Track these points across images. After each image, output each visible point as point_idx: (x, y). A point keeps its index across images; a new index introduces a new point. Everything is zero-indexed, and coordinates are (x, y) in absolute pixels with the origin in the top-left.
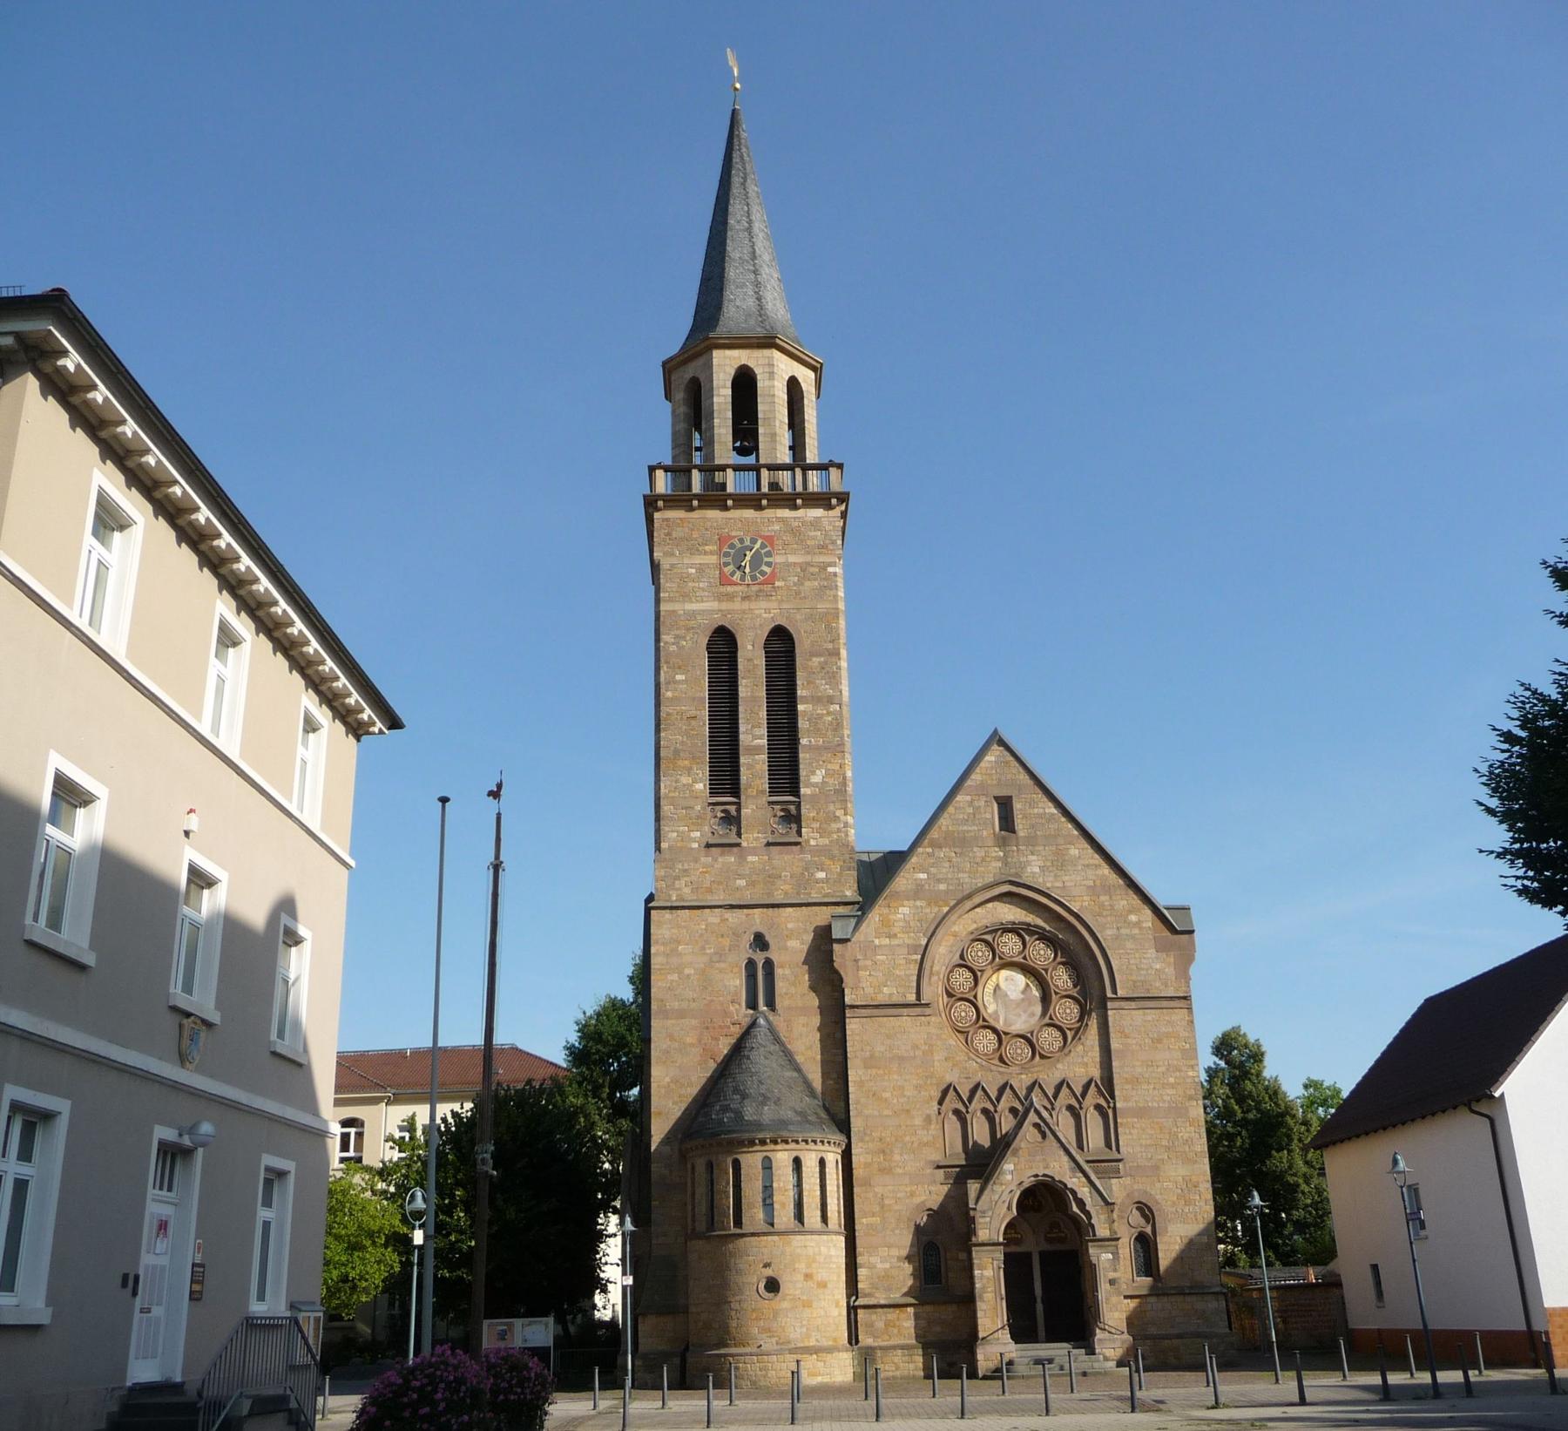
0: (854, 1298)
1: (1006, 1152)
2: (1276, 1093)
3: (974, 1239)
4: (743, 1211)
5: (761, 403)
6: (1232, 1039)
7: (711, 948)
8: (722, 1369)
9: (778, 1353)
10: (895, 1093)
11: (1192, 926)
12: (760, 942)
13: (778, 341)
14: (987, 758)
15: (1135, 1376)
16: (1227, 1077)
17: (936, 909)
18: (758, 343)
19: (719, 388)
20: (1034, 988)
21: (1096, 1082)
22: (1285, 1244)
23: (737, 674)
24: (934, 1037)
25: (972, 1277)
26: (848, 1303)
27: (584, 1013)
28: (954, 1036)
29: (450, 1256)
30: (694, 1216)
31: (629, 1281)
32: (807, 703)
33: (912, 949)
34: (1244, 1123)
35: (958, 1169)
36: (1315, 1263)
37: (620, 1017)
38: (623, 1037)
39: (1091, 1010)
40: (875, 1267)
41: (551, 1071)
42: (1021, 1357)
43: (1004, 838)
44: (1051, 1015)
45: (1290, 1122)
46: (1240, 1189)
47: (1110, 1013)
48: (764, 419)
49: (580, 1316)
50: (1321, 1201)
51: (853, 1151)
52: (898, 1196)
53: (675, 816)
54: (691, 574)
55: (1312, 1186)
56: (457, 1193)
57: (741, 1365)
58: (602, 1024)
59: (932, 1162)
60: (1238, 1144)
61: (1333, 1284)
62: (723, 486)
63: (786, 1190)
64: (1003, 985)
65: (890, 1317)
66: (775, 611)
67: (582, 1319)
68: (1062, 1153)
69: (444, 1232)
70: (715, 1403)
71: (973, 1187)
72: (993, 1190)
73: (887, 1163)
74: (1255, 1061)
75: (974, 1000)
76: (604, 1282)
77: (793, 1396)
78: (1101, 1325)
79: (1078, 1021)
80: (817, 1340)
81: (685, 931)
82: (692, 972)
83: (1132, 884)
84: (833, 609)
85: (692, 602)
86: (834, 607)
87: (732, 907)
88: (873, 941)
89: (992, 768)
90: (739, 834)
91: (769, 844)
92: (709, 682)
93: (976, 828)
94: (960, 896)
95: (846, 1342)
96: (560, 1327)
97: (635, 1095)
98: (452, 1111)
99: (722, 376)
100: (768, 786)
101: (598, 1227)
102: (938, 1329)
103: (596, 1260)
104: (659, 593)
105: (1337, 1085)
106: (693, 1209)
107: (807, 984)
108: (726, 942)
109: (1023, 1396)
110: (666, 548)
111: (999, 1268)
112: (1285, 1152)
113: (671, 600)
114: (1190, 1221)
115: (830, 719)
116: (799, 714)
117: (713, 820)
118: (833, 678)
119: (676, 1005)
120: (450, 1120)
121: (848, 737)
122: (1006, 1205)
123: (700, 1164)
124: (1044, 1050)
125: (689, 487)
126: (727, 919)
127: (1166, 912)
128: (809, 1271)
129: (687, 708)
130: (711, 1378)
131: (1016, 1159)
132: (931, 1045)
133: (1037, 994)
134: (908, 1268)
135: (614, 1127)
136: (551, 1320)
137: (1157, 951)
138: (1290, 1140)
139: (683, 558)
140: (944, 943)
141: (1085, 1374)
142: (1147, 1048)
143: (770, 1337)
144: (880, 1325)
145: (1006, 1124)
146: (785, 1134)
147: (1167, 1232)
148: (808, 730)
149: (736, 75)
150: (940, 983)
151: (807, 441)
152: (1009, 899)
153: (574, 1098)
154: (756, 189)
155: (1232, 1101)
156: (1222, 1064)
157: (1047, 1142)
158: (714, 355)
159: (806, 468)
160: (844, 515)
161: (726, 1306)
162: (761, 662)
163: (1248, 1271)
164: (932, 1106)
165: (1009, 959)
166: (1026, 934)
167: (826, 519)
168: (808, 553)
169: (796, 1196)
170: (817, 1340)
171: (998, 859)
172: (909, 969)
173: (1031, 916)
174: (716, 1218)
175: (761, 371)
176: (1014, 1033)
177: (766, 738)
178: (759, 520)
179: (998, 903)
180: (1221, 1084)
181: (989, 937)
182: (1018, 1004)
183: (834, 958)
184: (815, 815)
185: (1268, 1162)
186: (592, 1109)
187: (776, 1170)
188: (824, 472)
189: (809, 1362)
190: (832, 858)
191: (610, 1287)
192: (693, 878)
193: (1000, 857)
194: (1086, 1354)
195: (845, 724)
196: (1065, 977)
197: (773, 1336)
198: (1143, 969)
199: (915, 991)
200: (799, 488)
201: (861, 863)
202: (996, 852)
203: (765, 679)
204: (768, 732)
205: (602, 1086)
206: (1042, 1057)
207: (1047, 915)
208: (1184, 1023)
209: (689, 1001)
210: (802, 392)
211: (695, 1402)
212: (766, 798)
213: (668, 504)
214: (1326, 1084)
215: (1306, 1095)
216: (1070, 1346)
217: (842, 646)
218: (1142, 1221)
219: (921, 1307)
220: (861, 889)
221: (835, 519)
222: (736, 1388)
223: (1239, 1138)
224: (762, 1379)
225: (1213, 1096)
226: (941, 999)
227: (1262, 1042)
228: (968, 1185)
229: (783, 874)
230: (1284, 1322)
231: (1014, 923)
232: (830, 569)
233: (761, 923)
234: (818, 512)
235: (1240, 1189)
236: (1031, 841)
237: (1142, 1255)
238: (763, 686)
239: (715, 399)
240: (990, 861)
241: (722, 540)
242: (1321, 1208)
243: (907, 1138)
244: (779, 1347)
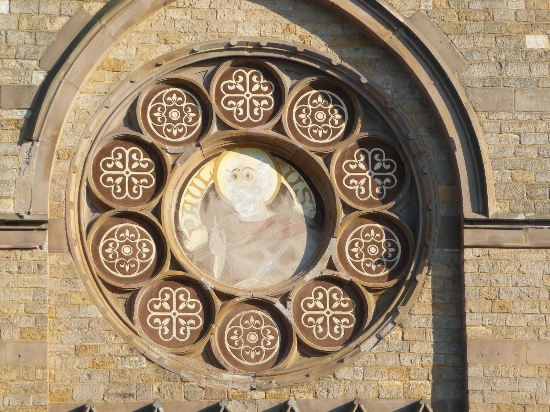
47: (468, 254)
75: (155, 220)
124: (313, 339)
150: (75, 179)
165: (242, 130)
166: (287, 72)
173: (298, 28)
207: (337, 29)
226: (73, 214)
231: (258, 47)
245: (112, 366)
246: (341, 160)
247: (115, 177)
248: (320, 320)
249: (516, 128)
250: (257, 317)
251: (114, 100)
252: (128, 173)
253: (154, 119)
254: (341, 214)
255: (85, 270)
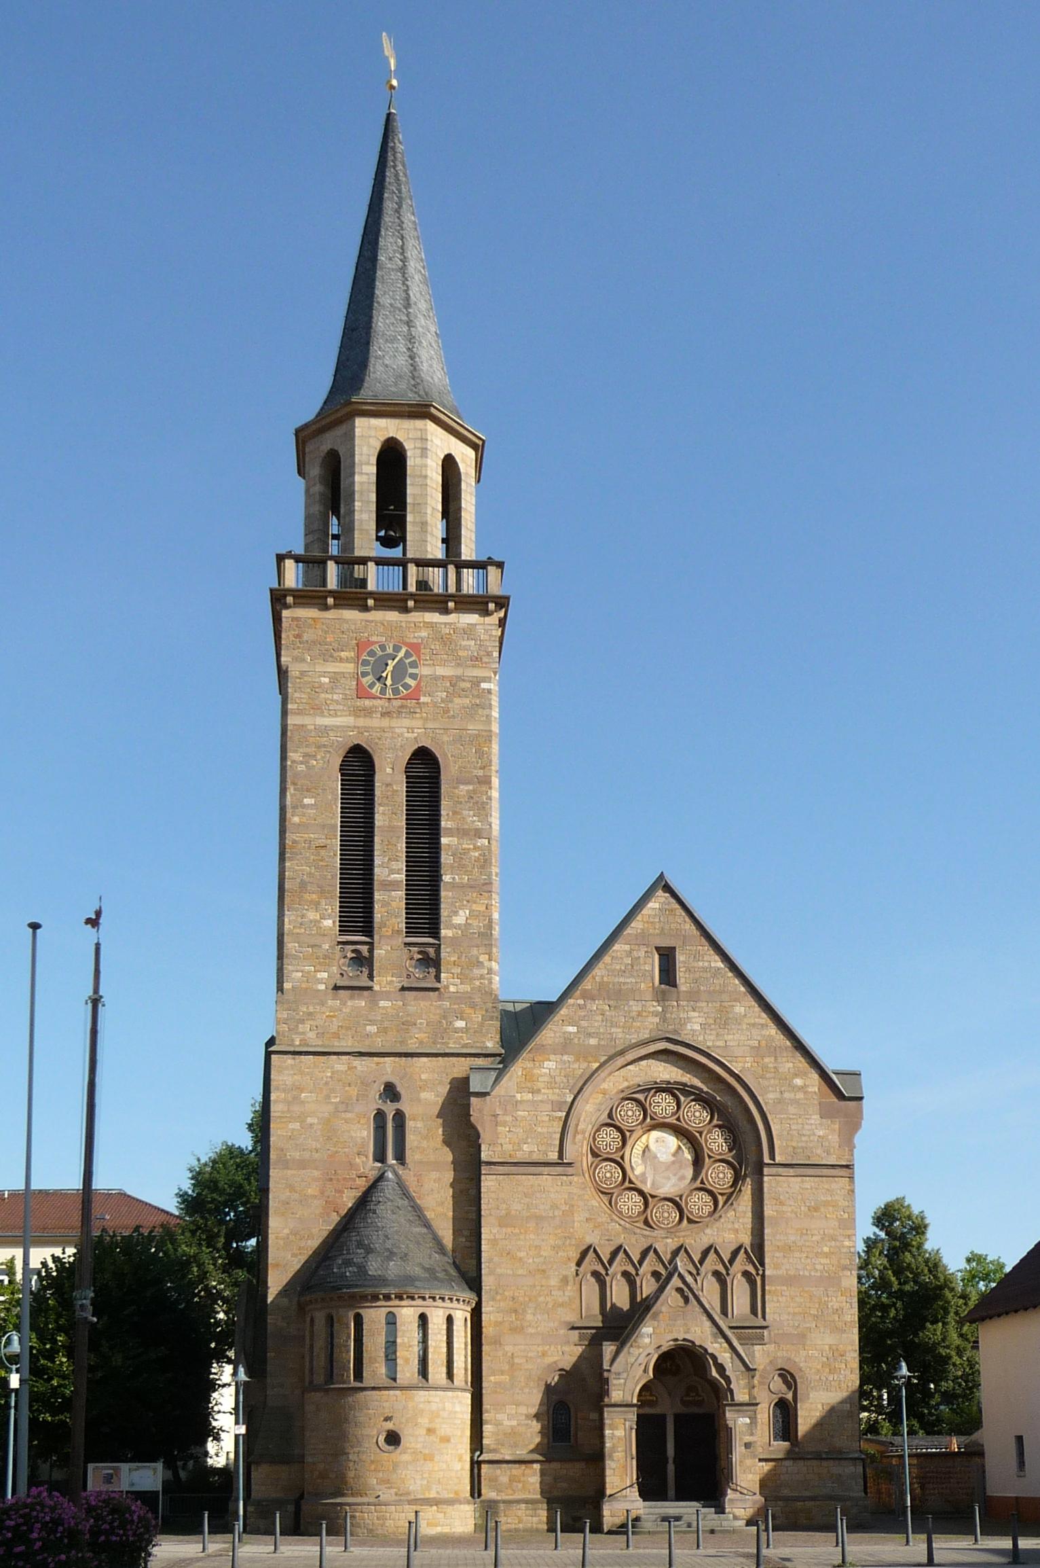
0: (478, 1453)
1: (646, 1316)
2: (936, 1265)
3: (606, 1400)
4: (364, 1366)
5: (412, 485)
6: (895, 1210)
7: (337, 1097)
8: (338, 1518)
9: (397, 1503)
10: (531, 1253)
11: (862, 1093)
12: (390, 1092)
13: (433, 410)
14: (650, 905)
15: (763, 1536)
16: (886, 1248)
17: (584, 1065)
18: (409, 412)
19: (361, 465)
20: (686, 1151)
21: (745, 1248)
22: (931, 1414)
23: (373, 800)
24: (576, 1198)
25: (602, 1437)
26: (472, 1459)
27: (199, 1160)
28: (597, 1197)
29: (52, 1400)
30: (311, 1370)
31: (242, 1430)
32: (452, 836)
33: (557, 1106)
34: (900, 1295)
35: (594, 1331)
36: (959, 1432)
37: (238, 1166)
38: (241, 1186)
39: (746, 1176)
40: (502, 1424)
41: (163, 1217)
42: (648, 1514)
43: (663, 992)
44: (702, 1180)
45: (948, 1295)
46: (890, 1359)
47: (766, 1179)
48: (414, 504)
49: (192, 1462)
50: (973, 1374)
51: (483, 1310)
52: (529, 1355)
53: (301, 955)
54: (324, 684)
55: (965, 1359)
56: (59, 1338)
57: (357, 1514)
58: (218, 1173)
59: (568, 1323)
60: (892, 1315)
61: (975, 1453)
62: (364, 582)
63: (410, 1346)
64: (653, 1147)
65: (515, 1472)
66: (419, 731)
67: (194, 1466)
68: (705, 1318)
69: (46, 1377)
70: (328, 1550)
71: (609, 1349)
72: (629, 1353)
73: (518, 1322)
74: (918, 1233)
75: (621, 1161)
76: (216, 1431)
77: (409, 1545)
78: (733, 1486)
79: (731, 1187)
80: (438, 1493)
81: (308, 1077)
82: (316, 1121)
83: (800, 1046)
84: (485, 731)
85: (324, 716)
86: (488, 728)
87: (361, 1054)
88: (514, 1096)
89: (656, 915)
90: (371, 977)
91: (403, 989)
92: (342, 808)
93: (634, 981)
94: (612, 1051)
95: (468, 1494)
96: (169, 1474)
97: (253, 1246)
98: (53, 1256)
99: (365, 449)
100: (404, 925)
101: (212, 1376)
102: (564, 1485)
103: (208, 1408)
104: (287, 704)
105: (1001, 1260)
106: (311, 1361)
107: (442, 1137)
108: (353, 1091)
109: (647, 1551)
110: (296, 652)
111: (632, 1429)
112: (940, 1324)
113: (300, 712)
114: (833, 1389)
115: (477, 854)
116: (443, 847)
117: (343, 960)
118: (482, 809)
119: (297, 1155)
120: (51, 1265)
121: (496, 876)
122: (643, 1367)
123: (320, 1317)
125: (324, 582)
126: (355, 1067)
127: (834, 1077)
128: (430, 1426)
129: (316, 836)
130: (324, 1526)
131: (656, 1322)
132: (573, 1206)
133: (690, 1158)
134: (536, 1426)
135: (229, 1277)
136: (159, 1466)
137: (821, 1118)
138: (946, 1312)
139: (314, 664)
140: (591, 1101)
141: (712, 1532)
142: (802, 1216)
143: (389, 1488)
144: (504, 1479)
145: (647, 1287)
146: (411, 1290)
147: (808, 1398)
148: (452, 867)
149: (393, 69)
150: (585, 1142)
151: (463, 532)
152: (664, 1057)
153: (187, 1246)
154: (413, 218)
155: (890, 1272)
156: (882, 1235)
157: (689, 1307)
158: (357, 424)
159: (461, 565)
160: (502, 623)
161: (345, 1457)
162: (401, 787)
163: (889, 1438)
164: (571, 1268)
165: (662, 1120)
167: (481, 627)
168: (459, 665)
169: (421, 1352)
170: (438, 1493)
171: (655, 1014)
172: (552, 1126)
173: (688, 1075)
174: (335, 1371)
175: (412, 446)
176: (662, 1196)
177: (405, 873)
178: (404, 624)
179: (653, 1061)
180: (880, 1255)
181: (641, 1097)
182: (668, 1166)
183: (471, 1113)
184: (456, 959)
185: (921, 1334)
186: (206, 1258)
187: (401, 1325)
188: (481, 571)
189: (428, 1513)
190: (473, 1006)
191: (223, 1435)
192: (320, 1022)
193: (657, 1011)
194: (716, 1513)
195: (493, 861)
196: (721, 1140)
197: (391, 1488)
198: (804, 1135)
199: (557, 1149)
200: (452, 589)
201: (505, 1014)
202: (653, 1006)
203: (405, 808)
204: (407, 866)
205: (218, 1235)
206: (690, 1221)
208: (844, 1192)
209: (311, 1152)
210: (459, 474)
211: (308, 1548)
212: (403, 938)
213: (297, 601)
214: (989, 1259)
215: (968, 1268)
216: (698, 1505)
217: (493, 774)
218: (784, 1388)
219: (547, 1464)
220: (503, 1042)
221: (493, 628)
222: (352, 1535)
223: (893, 1309)
224: (380, 1527)
225: (870, 1266)
226: (585, 1158)
227: (926, 1214)
228: (604, 1347)
229: (418, 1021)
230: (922, 1487)
231: (669, 1083)
232: (484, 685)
233: (392, 1072)
234: (472, 618)
235: (890, 1359)
236: (693, 996)
237: (780, 1420)
238: (402, 816)
239: (357, 478)
240: (647, 1016)
241: (360, 646)
242: (971, 1381)
243: (541, 1299)
244: (397, 1498)
245: (603, 1227)
246: (707, 1134)
247: (603, 1141)
248: (697, 1207)
249: (788, 1121)
250: (668, 1205)
251: (603, 1107)
252: (608, 1139)
253: (620, 1115)
254: (707, 1159)
255: (590, 1185)
